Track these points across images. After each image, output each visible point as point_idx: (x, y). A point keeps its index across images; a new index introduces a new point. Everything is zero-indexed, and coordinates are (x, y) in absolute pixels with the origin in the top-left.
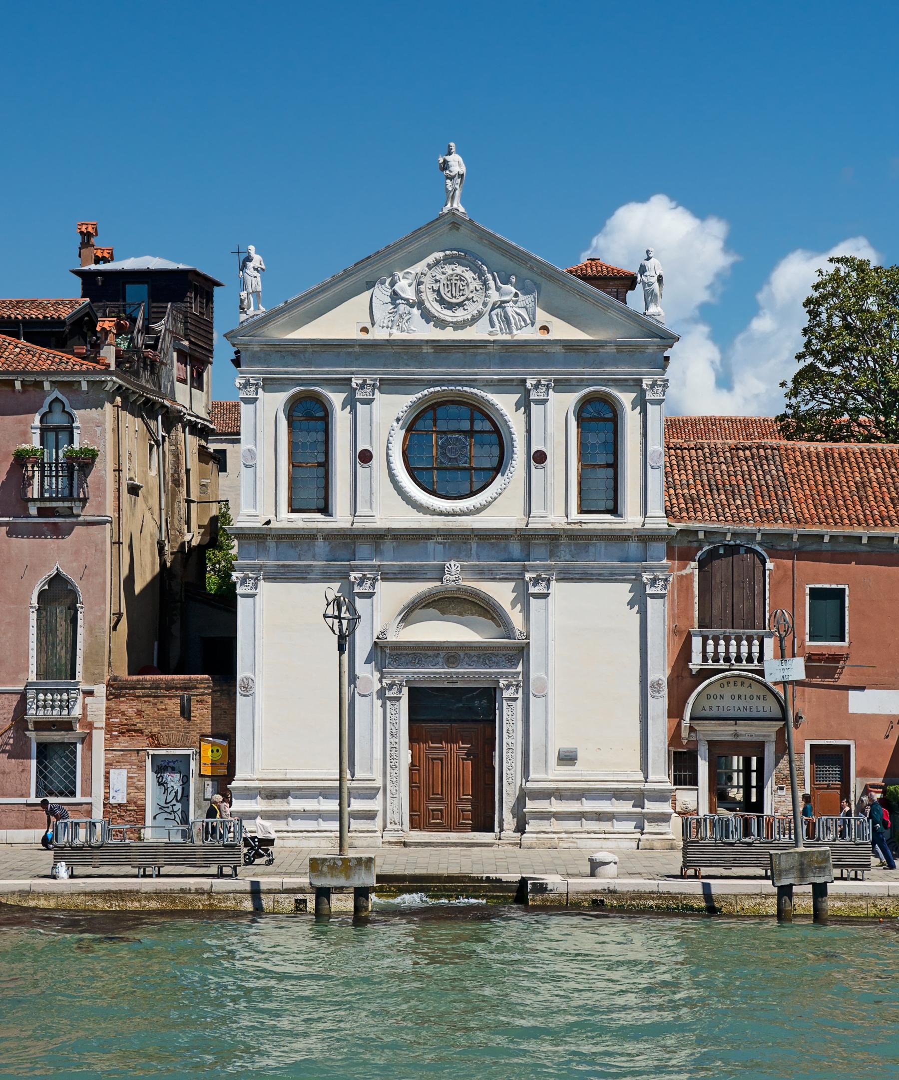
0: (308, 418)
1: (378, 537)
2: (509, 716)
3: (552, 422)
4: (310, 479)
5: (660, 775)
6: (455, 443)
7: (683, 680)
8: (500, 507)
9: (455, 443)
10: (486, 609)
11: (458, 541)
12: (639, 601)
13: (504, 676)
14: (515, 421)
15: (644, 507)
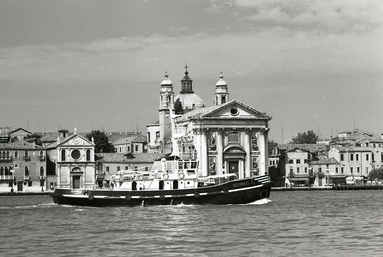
6: (76, 154)
9: (76, 154)
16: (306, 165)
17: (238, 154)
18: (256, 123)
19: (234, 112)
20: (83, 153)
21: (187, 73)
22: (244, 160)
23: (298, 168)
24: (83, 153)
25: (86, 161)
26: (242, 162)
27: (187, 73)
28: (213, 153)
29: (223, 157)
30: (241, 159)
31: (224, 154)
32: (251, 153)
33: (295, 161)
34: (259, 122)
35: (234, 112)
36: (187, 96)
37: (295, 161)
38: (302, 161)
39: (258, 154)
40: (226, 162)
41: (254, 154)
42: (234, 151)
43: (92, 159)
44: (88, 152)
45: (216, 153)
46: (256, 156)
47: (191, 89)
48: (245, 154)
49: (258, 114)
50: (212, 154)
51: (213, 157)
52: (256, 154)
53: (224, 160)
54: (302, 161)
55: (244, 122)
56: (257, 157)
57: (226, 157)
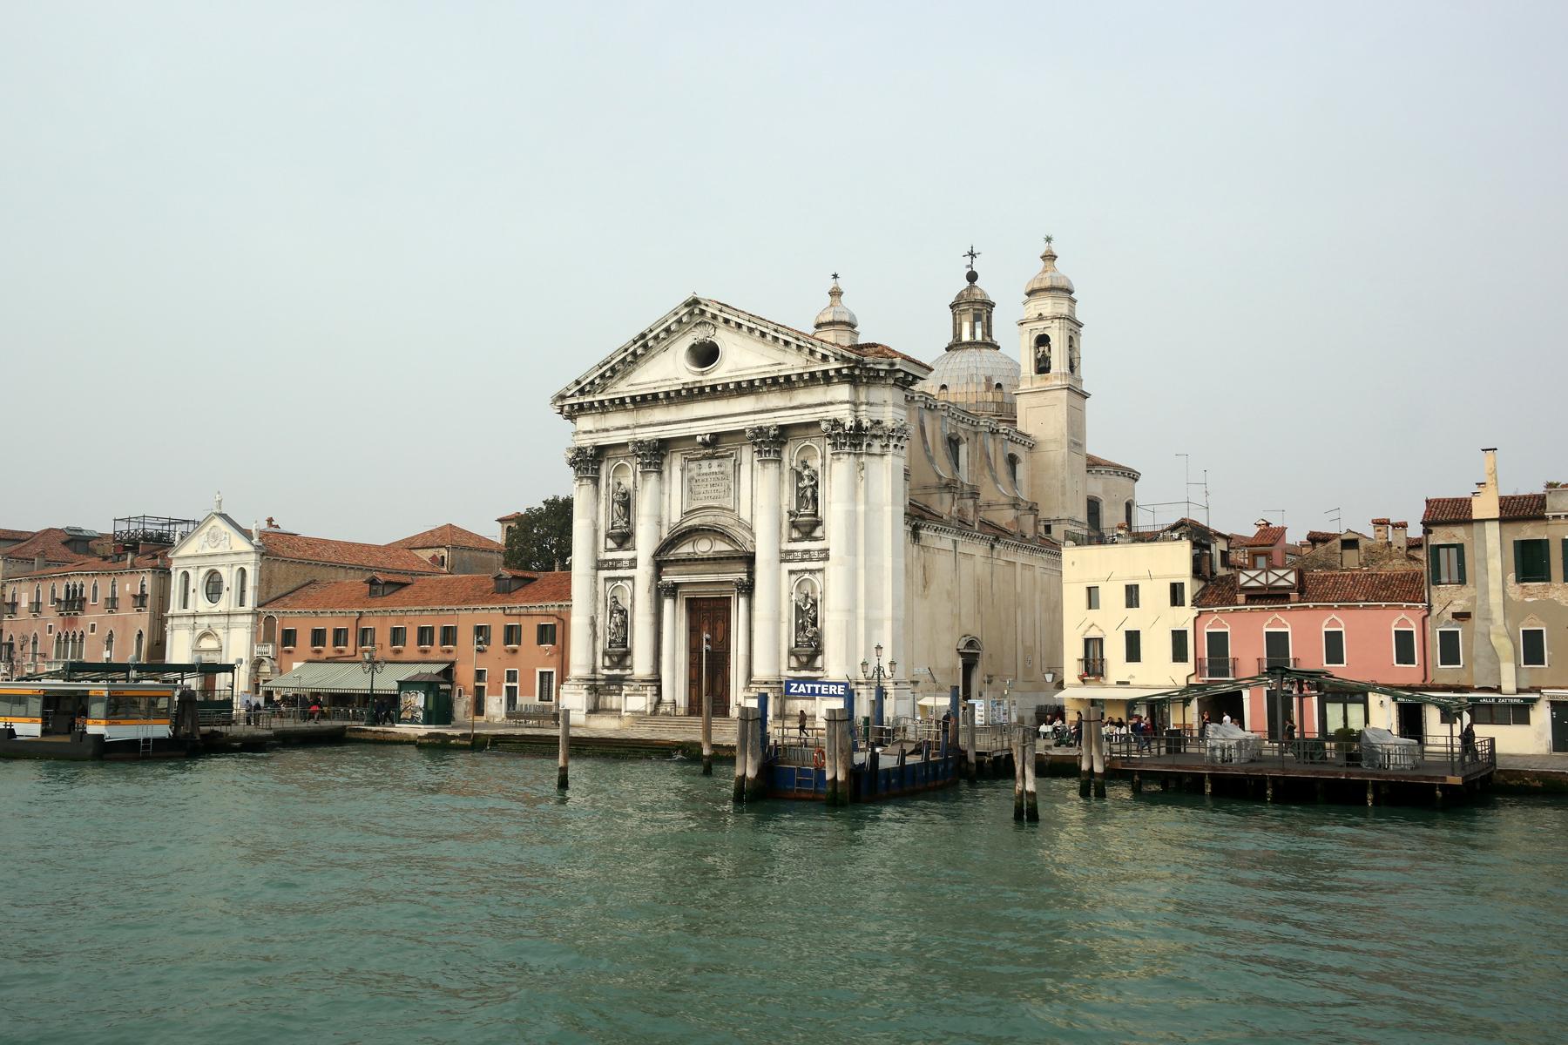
6: (214, 587)
9: (214, 587)
16: (1184, 617)
17: (717, 560)
18: (802, 397)
19: (706, 355)
20: (229, 578)
21: (972, 277)
22: (748, 589)
23: (1133, 639)
26: (742, 601)
27: (972, 277)
28: (621, 560)
29: (658, 574)
31: (659, 565)
32: (785, 557)
38: (1155, 594)
39: (819, 560)
40: (668, 604)
41: (802, 560)
42: (703, 547)
43: (250, 604)
45: (633, 563)
46: (811, 571)
47: (990, 336)
48: (749, 560)
50: (616, 568)
51: (622, 579)
52: (811, 560)
53: (662, 592)
56: (818, 575)
57: (665, 579)
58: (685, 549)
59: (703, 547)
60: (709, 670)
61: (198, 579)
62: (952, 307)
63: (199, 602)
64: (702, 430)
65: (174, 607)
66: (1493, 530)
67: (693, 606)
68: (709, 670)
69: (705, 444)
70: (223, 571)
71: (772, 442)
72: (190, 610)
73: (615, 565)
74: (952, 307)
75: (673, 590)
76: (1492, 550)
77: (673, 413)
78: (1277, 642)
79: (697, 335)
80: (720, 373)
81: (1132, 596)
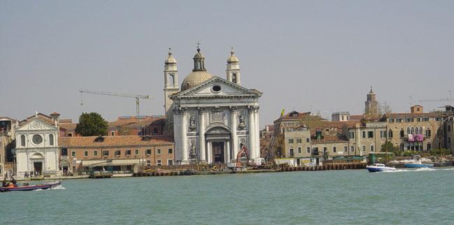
0: (23, 137)
1: (30, 149)
2: (43, 164)
3: (47, 136)
4: (23, 143)
5: (58, 170)
6: (37, 139)
7: (60, 160)
8: (41, 145)
9: (37, 139)
10: (40, 154)
11: (38, 148)
12: (56, 153)
13: (43, 161)
14: (43, 137)
15: (56, 144)
17: (222, 135)
18: (242, 100)
19: (217, 89)
20: (46, 137)
21: (199, 50)
22: (231, 140)
24: (46, 137)
25: (48, 145)
26: (228, 143)
27: (199, 50)
29: (206, 138)
30: (227, 140)
31: (206, 135)
32: (238, 133)
33: (295, 141)
34: (246, 100)
35: (217, 89)
36: (197, 74)
37: (295, 141)
38: (304, 140)
40: (208, 144)
42: (218, 132)
43: (56, 144)
44: (51, 136)
48: (230, 135)
49: (245, 91)
53: (206, 142)
54: (304, 140)
55: (229, 100)
58: (213, 132)
59: (218, 132)
60: (219, 158)
61: (30, 137)
62: (194, 59)
63: (30, 143)
64: (217, 106)
65: (19, 145)
66: (359, 130)
67: (215, 144)
68: (219, 158)
69: (217, 109)
70: (42, 135)
71: (231, 110)
72: (26, 147)
73: (192, 135)
74: (194, 59)
75: (209, 140)
76: (359, 132)
77: (209, 101)
78: (325, 149)
79: (217, 84)
80: (221, 93)
81: (300, 141)
